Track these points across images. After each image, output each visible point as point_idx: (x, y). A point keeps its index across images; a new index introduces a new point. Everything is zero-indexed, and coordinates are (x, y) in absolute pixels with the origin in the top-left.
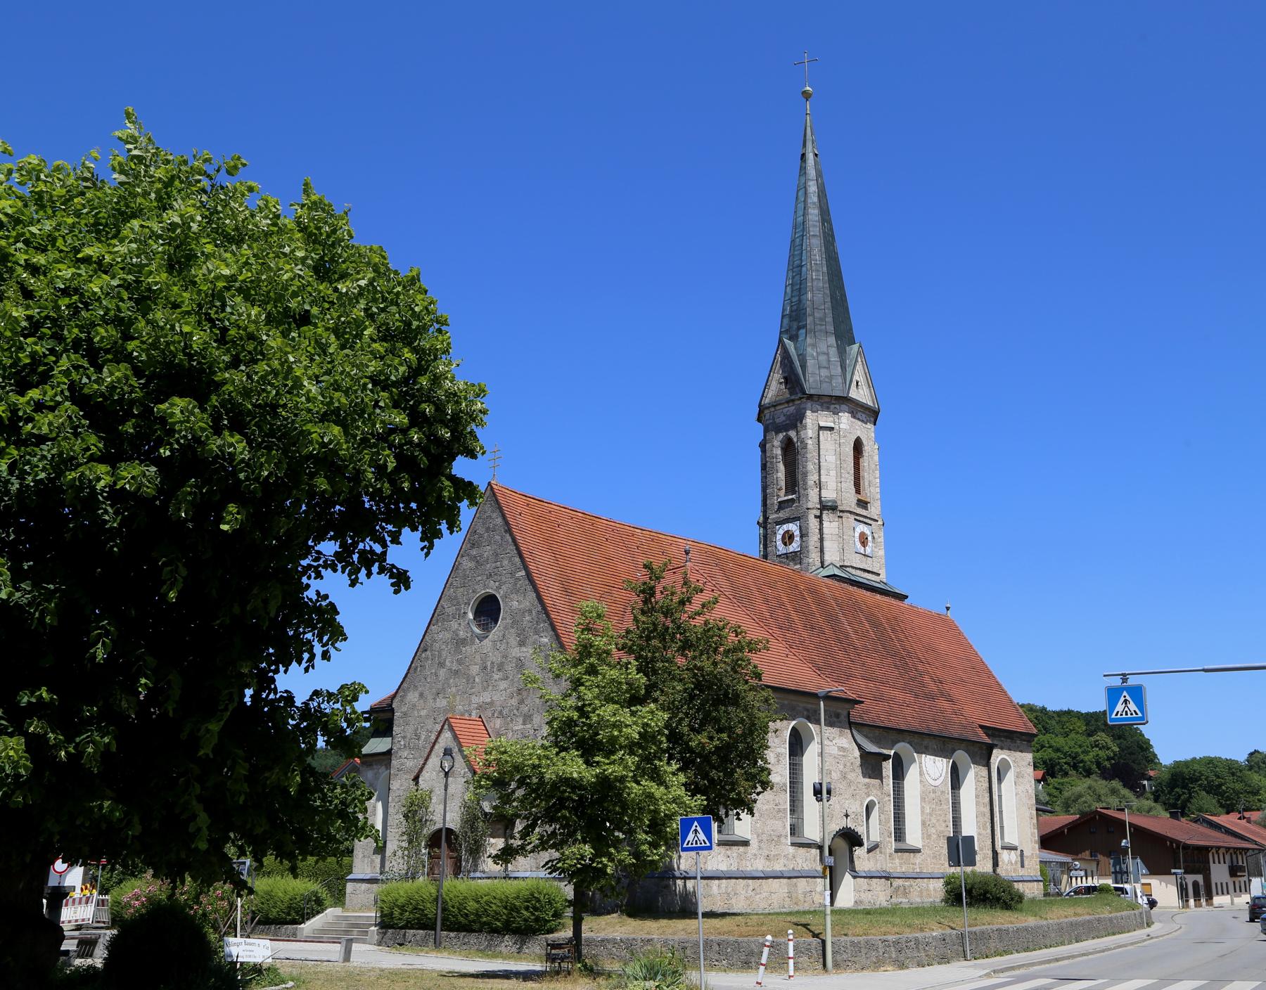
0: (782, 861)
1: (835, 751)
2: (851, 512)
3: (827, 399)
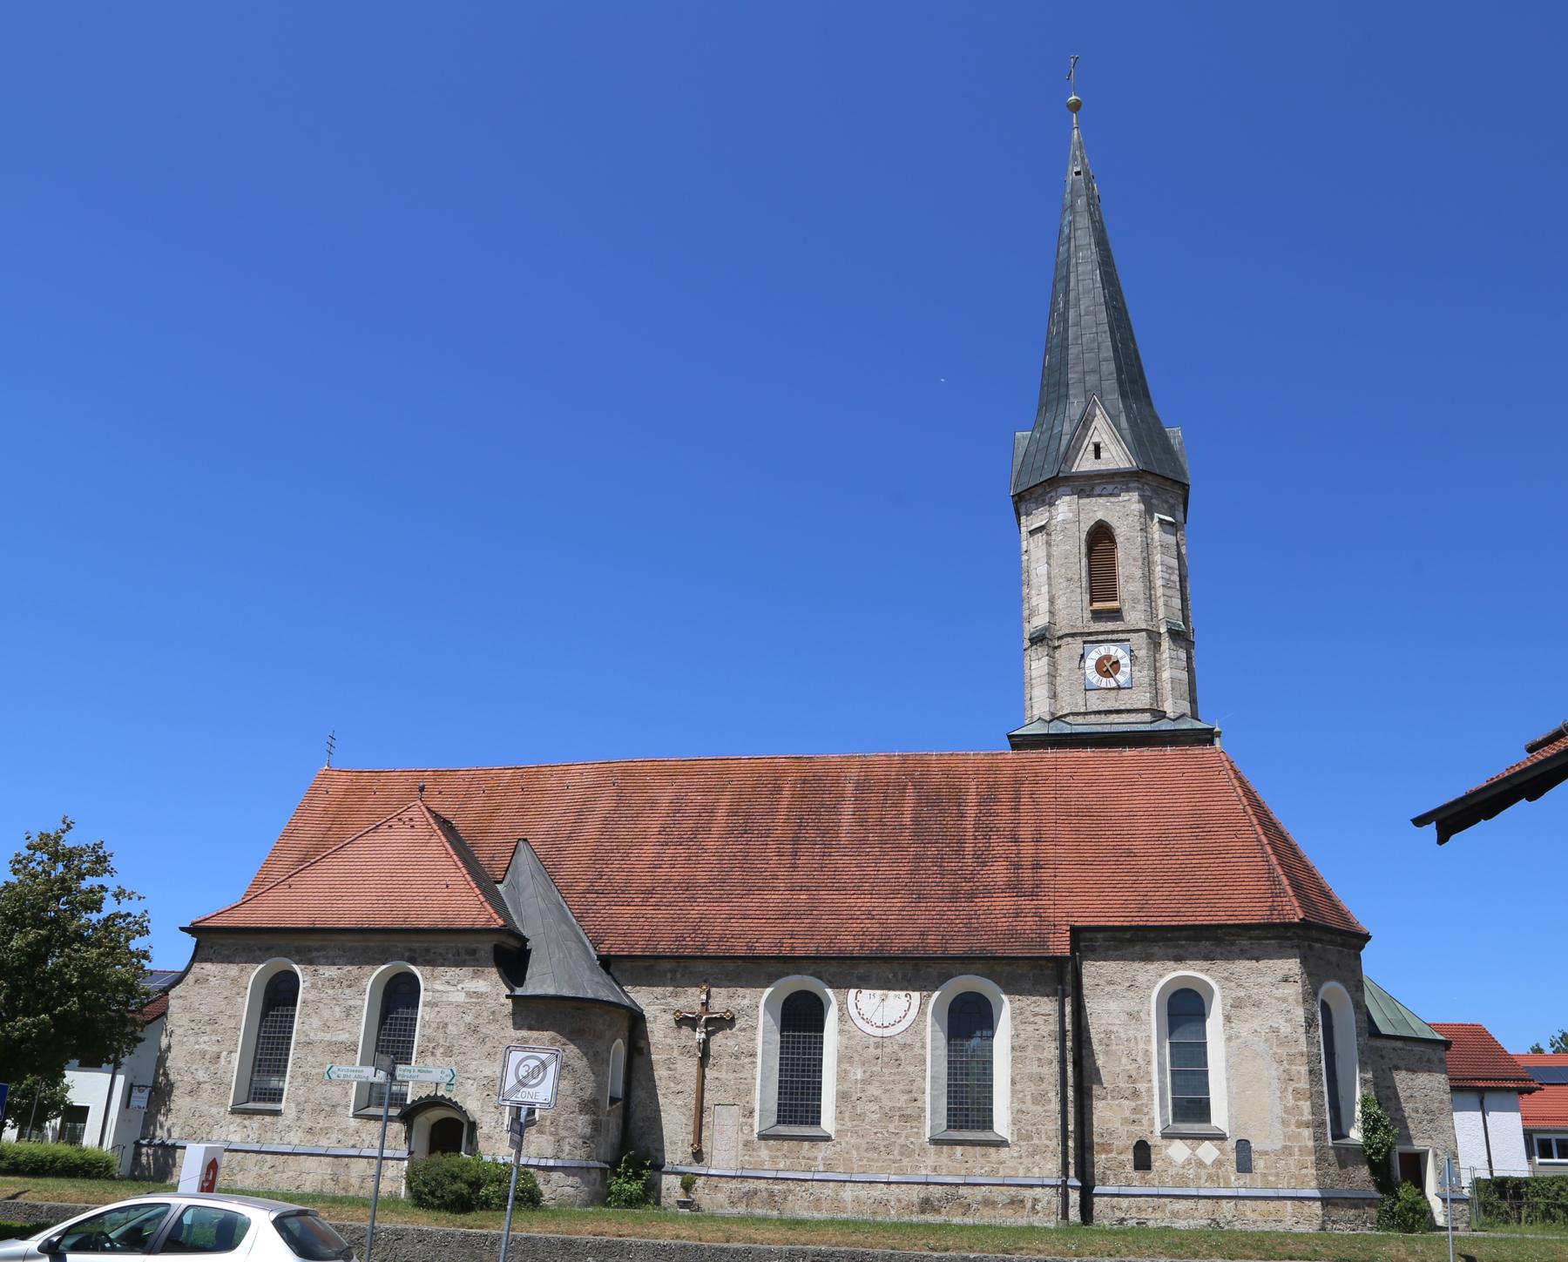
0: (334, 1136)
1: (460, 997)
2: (1073, 635)
3: (1040, 490)
